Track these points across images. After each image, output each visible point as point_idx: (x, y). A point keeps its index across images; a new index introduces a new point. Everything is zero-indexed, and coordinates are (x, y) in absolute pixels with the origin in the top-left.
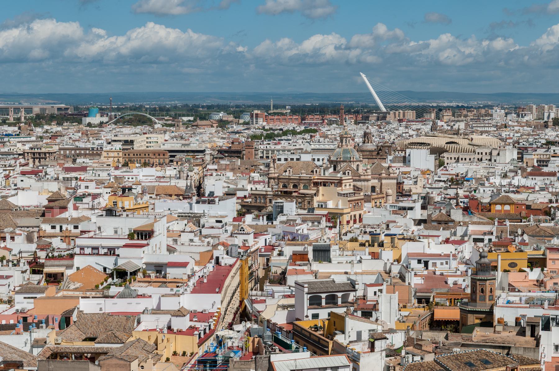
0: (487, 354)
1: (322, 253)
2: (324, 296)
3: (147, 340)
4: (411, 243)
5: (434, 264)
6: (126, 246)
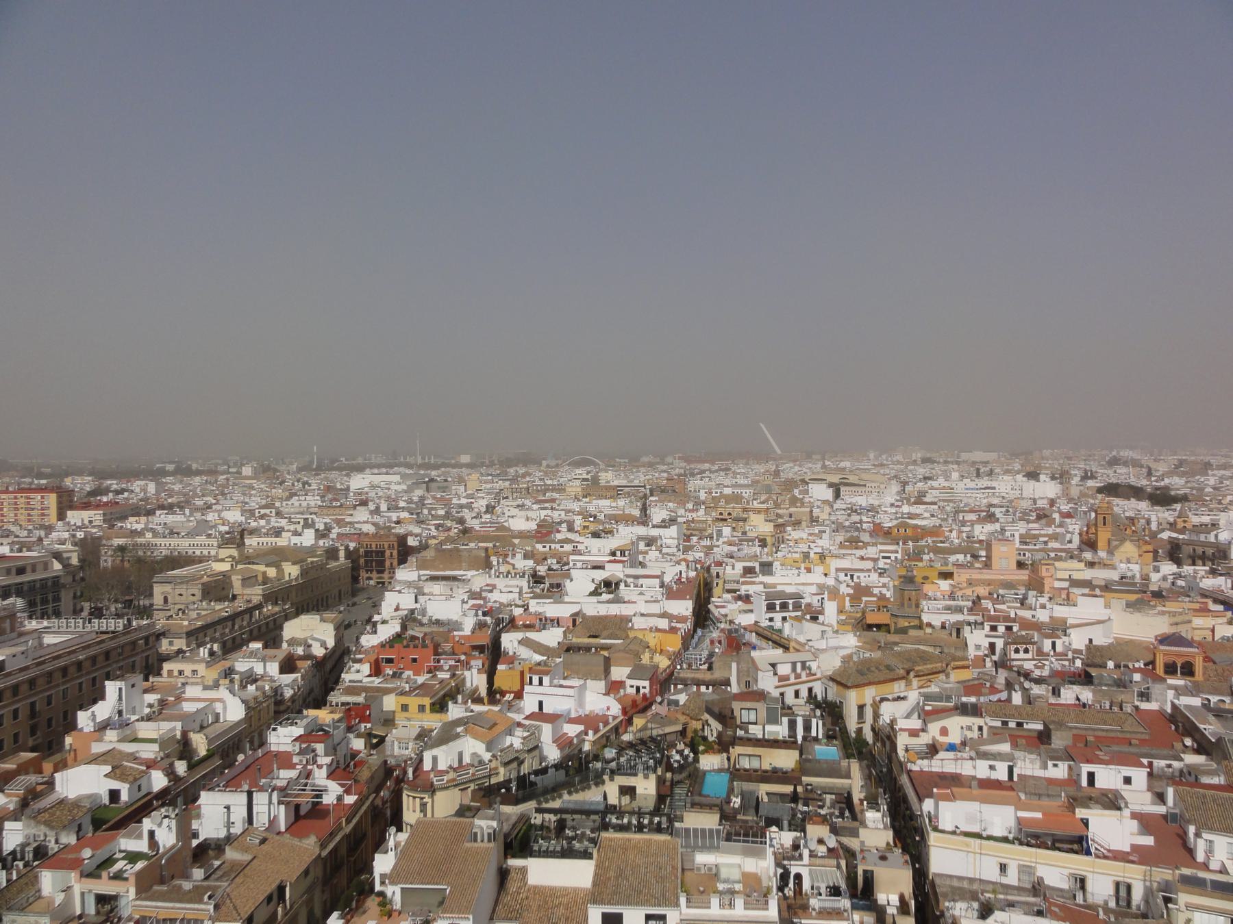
0: (924, 652)
1: (767, 568)
2: (778, 602)
4: (838, 560)
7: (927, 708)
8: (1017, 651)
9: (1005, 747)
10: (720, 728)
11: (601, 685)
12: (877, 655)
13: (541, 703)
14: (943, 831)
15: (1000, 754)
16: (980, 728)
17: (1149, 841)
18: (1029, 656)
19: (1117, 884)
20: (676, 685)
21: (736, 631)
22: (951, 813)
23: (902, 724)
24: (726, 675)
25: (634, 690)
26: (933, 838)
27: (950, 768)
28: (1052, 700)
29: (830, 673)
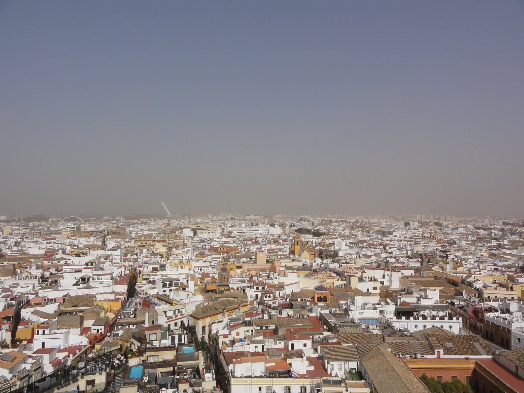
0: (230, 300)
1: (163, 267)
2: (168, 283)
3: (100, 304)
5: (204, 270)
6: (84, 268)
7: (231, 324)
8: (266, 297)
9: (261, 338)
10: (139, 344)
11: (78, 331)
12: (211, 303)
13: (43, 344)
14: (237, 378)
15: (259, 341)
16: (252, 331)
17: (312, 368)
18: (271, 299)
19: (301, 388)
20: (117, 326)
21: (148, 297)
22: (239, 369)
23: (221, 333)
24: (143, 319)
25: (96, 331)
26: (233, 381)
27: (240, 349)
28: (279, 316)
29: (190, 313)
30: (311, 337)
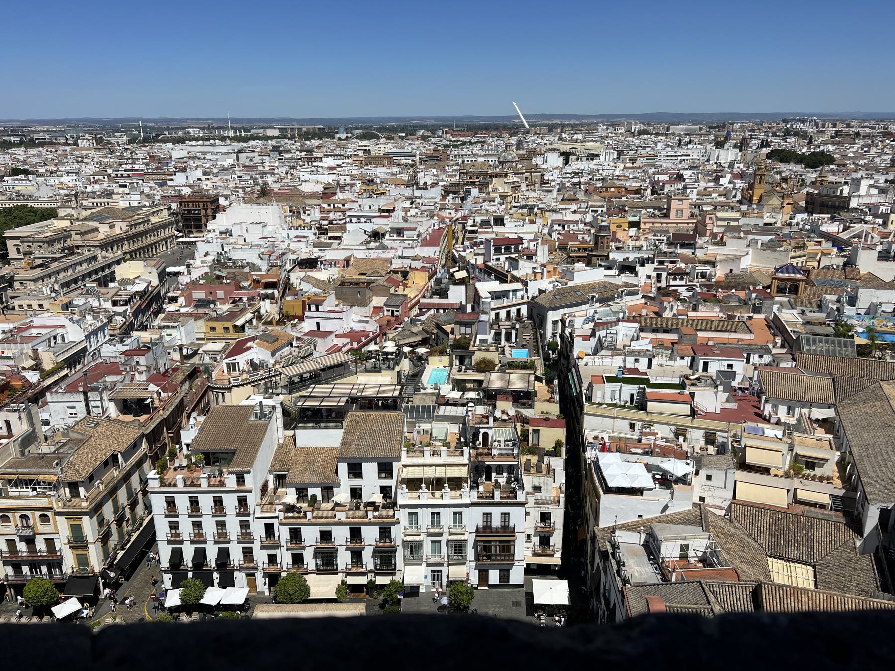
1: (499, 221)
8: (675, 279)
13: (318, 323)
17: (733, 405)
25: (390, 313)
30: (745, 355)
